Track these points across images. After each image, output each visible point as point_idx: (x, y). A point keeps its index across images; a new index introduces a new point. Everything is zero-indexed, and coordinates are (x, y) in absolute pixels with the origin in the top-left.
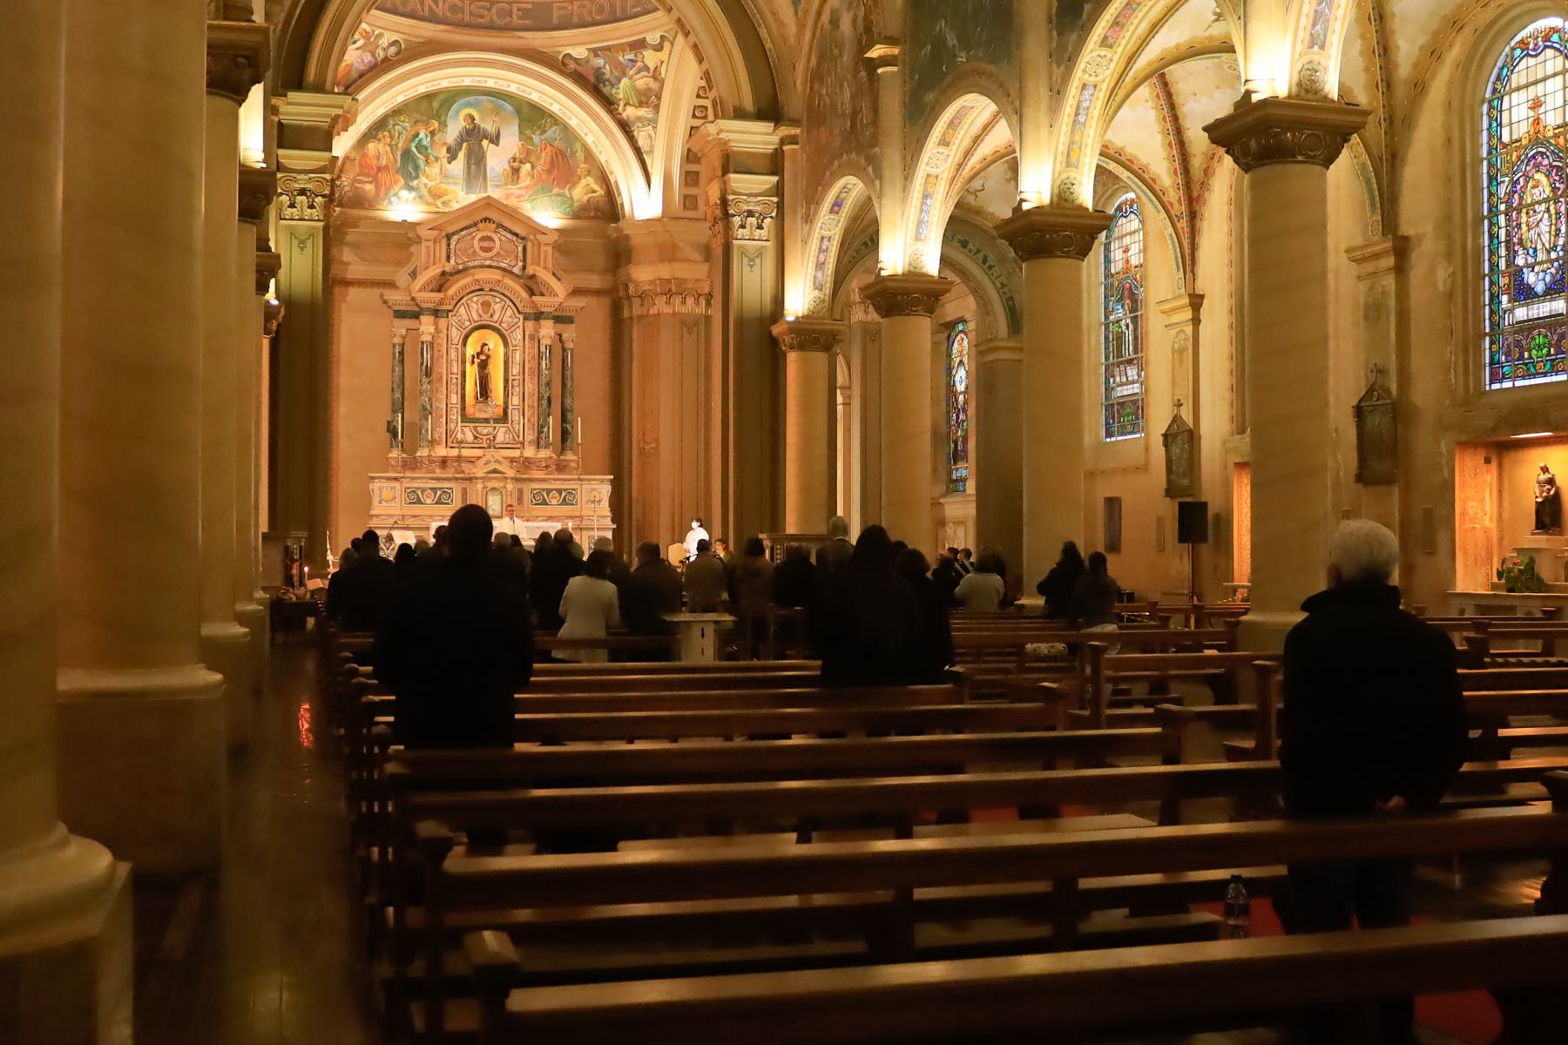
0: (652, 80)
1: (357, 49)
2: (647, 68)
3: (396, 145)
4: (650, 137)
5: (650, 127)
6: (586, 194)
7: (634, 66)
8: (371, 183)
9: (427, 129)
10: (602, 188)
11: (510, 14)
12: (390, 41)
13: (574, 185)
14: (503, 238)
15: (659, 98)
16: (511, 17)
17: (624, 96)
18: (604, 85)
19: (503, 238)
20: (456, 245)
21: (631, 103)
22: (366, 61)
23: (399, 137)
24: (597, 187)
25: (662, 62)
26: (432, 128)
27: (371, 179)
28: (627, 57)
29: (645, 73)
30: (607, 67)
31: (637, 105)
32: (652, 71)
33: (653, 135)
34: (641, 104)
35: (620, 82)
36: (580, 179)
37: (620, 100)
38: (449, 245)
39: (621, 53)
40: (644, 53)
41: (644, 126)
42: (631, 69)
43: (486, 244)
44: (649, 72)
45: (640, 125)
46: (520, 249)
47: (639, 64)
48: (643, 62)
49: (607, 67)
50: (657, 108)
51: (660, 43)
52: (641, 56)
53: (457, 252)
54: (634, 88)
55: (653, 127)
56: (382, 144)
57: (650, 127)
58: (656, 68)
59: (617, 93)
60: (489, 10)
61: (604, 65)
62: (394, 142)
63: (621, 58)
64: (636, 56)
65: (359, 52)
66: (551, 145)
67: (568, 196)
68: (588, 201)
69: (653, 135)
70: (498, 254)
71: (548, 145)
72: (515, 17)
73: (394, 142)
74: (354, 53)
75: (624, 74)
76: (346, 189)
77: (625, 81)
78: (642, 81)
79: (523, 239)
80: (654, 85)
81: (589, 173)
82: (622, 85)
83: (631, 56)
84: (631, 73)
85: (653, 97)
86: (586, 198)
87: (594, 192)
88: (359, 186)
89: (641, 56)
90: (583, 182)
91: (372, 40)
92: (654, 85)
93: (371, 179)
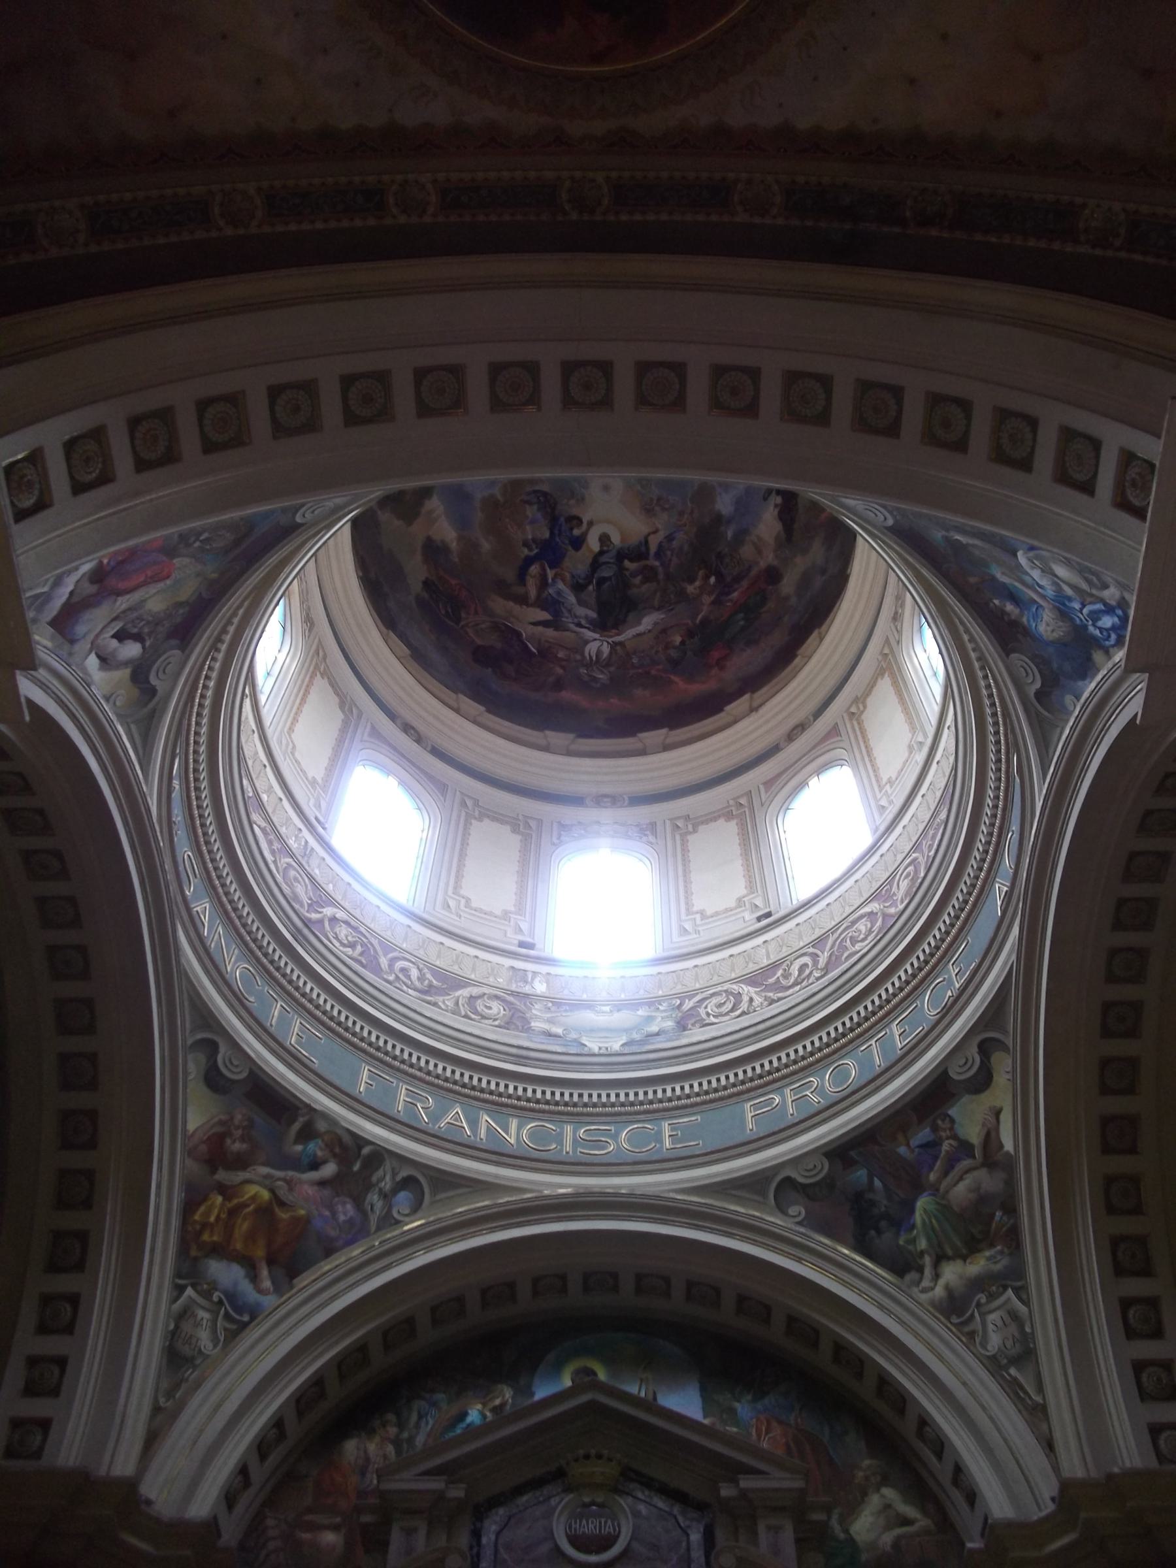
0: (982, 1174)
1: (322, 1183)
2: (965, 1148)
3: (411, 1440)
4: (1014, 1316)
5: (1010, 1292)
6: (888, 1527)
7: (936, 1158)
8: (335, 1528)
9: (484, 1405)
10: (925, 1513)
11: (658, 1137)
12: (399, 1178)
13: (852, 1510)
14: (642, 1508)
15: (1011, 1209)
16: (660, 1140)
17: (929, 1239)
18: (879, 1232)
19: (642, 1508)
20: (498, 1534)
21: (950, 1252)
22: (342, 1218)
23: (417, 1426)
24: (910, 1511)
25: (998, 1113)
26: (497, 1402)
27: (338, 1520)
28: (914, 1142)
29: (966, 1163)
30: (877, 1183)
31: (964, 1251)
32: (978, 1153)
33: (1022, 1309)
34: (972, 1247)
35: (912, 1211)
36: (865, 1494)
37: (922, 1253)
38: (477, 1534)
39: (900, 1137)
40: (950, 1112)
41: (992, 1297)
42: (931, 1168)
43: (589, 1527)
44: (974, 1157)
45: (983, 1298)
46: (696, 1537)
47: (946, 1146)
48: (955, 1137)
49: (877, 1183)
50: (1013, 1239)
51: (982, 1061)
52: (947, 1125)
53: (504, 1554)
54: (945, 1209)
55: (1017, 1290)
56: (377, 1439)
57: (1010, 1292)
58: (988, 1135)
59: (913, 1241)
60: (615, 1137)
61: (871, 1182)
62: (405, 1435)
63: (902, 1150)
64: (935, 1129)
65: (327, 1192)
66: (780, 1422)
67: (842, 1536)
68: (896, 1545)
69: (1022, 1309)
70: (625, 1553)
71: (775, 1424)
72: (667, 1143)
73: (405, 1435)
74: (311, 1191)
75: (917, 1187)
76: (271, 1545)
77: (923, 1203)
78: (961, 1187)
79: (701, 1507)
80: (989, 1181)
81: (885, 1481)
82: (918, 1217)
83: (923, 1135)
84: (932, 1177)
85: (998, 1214)
86: (888, 1539)
87: (906, 1522)
88: (306, 1536)
89: (947, 1125)
90: (875, 1501)
91: (356, 1167)
92: (989, 1181)
93: (338, 1520)
